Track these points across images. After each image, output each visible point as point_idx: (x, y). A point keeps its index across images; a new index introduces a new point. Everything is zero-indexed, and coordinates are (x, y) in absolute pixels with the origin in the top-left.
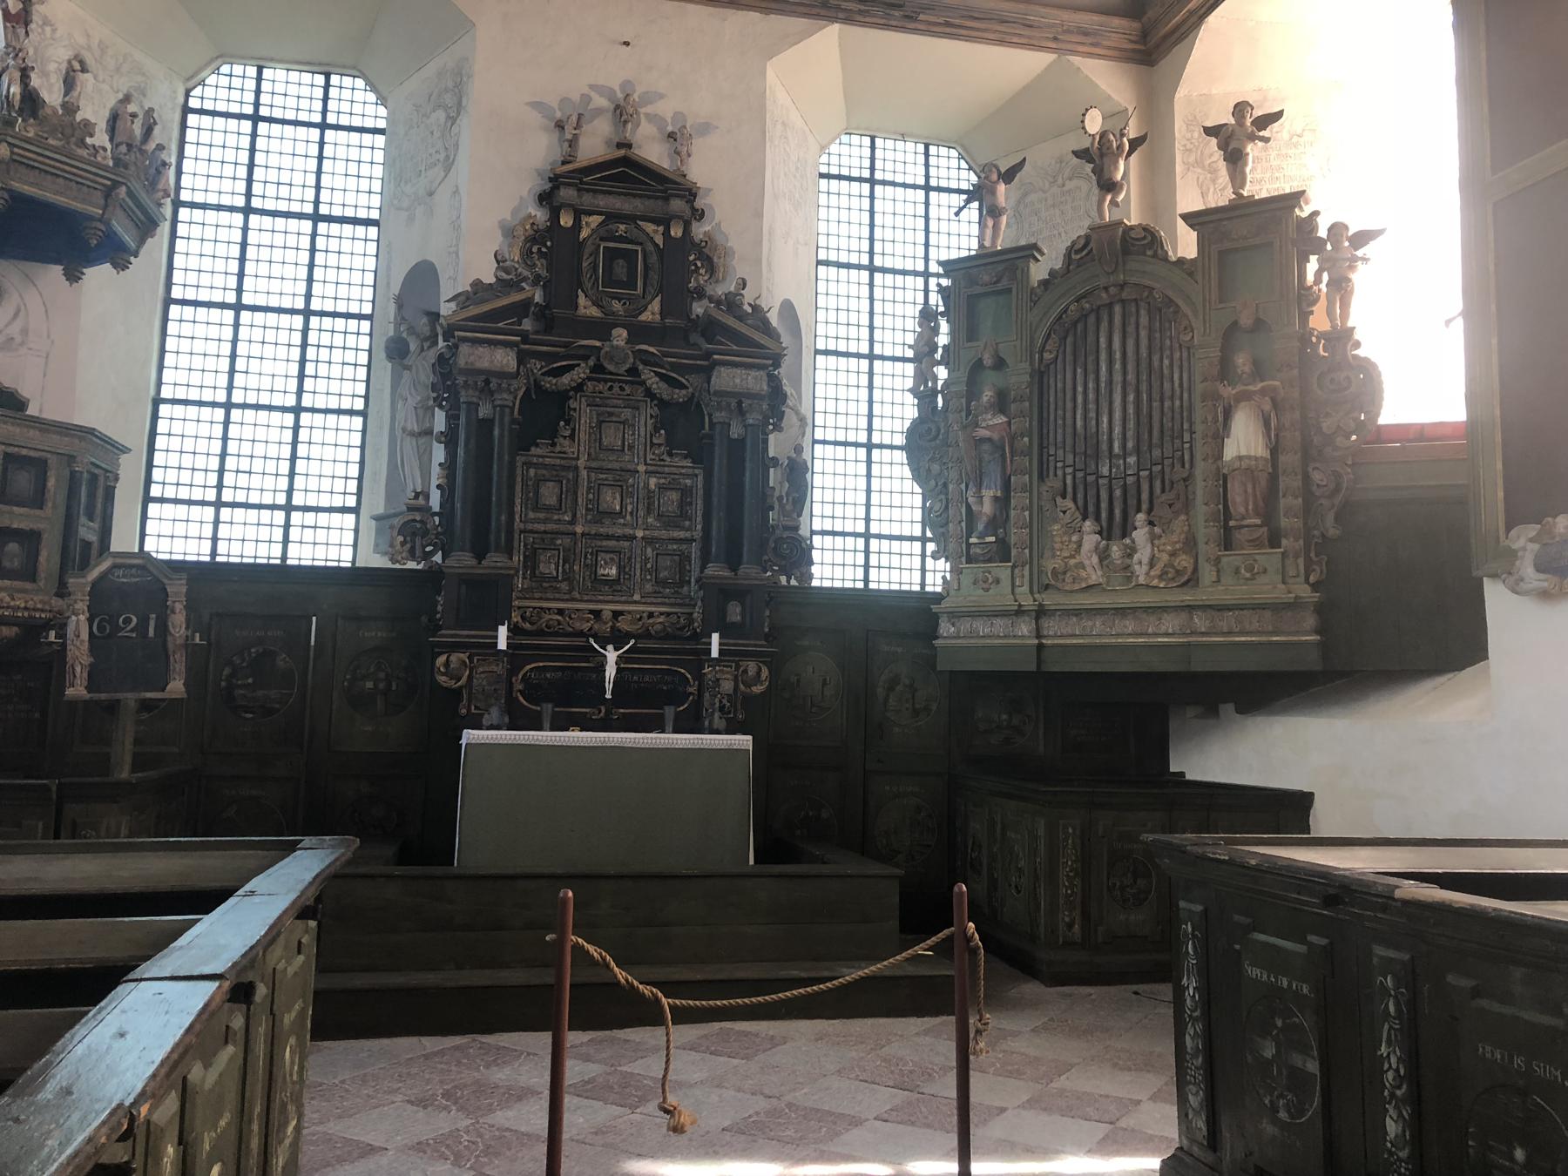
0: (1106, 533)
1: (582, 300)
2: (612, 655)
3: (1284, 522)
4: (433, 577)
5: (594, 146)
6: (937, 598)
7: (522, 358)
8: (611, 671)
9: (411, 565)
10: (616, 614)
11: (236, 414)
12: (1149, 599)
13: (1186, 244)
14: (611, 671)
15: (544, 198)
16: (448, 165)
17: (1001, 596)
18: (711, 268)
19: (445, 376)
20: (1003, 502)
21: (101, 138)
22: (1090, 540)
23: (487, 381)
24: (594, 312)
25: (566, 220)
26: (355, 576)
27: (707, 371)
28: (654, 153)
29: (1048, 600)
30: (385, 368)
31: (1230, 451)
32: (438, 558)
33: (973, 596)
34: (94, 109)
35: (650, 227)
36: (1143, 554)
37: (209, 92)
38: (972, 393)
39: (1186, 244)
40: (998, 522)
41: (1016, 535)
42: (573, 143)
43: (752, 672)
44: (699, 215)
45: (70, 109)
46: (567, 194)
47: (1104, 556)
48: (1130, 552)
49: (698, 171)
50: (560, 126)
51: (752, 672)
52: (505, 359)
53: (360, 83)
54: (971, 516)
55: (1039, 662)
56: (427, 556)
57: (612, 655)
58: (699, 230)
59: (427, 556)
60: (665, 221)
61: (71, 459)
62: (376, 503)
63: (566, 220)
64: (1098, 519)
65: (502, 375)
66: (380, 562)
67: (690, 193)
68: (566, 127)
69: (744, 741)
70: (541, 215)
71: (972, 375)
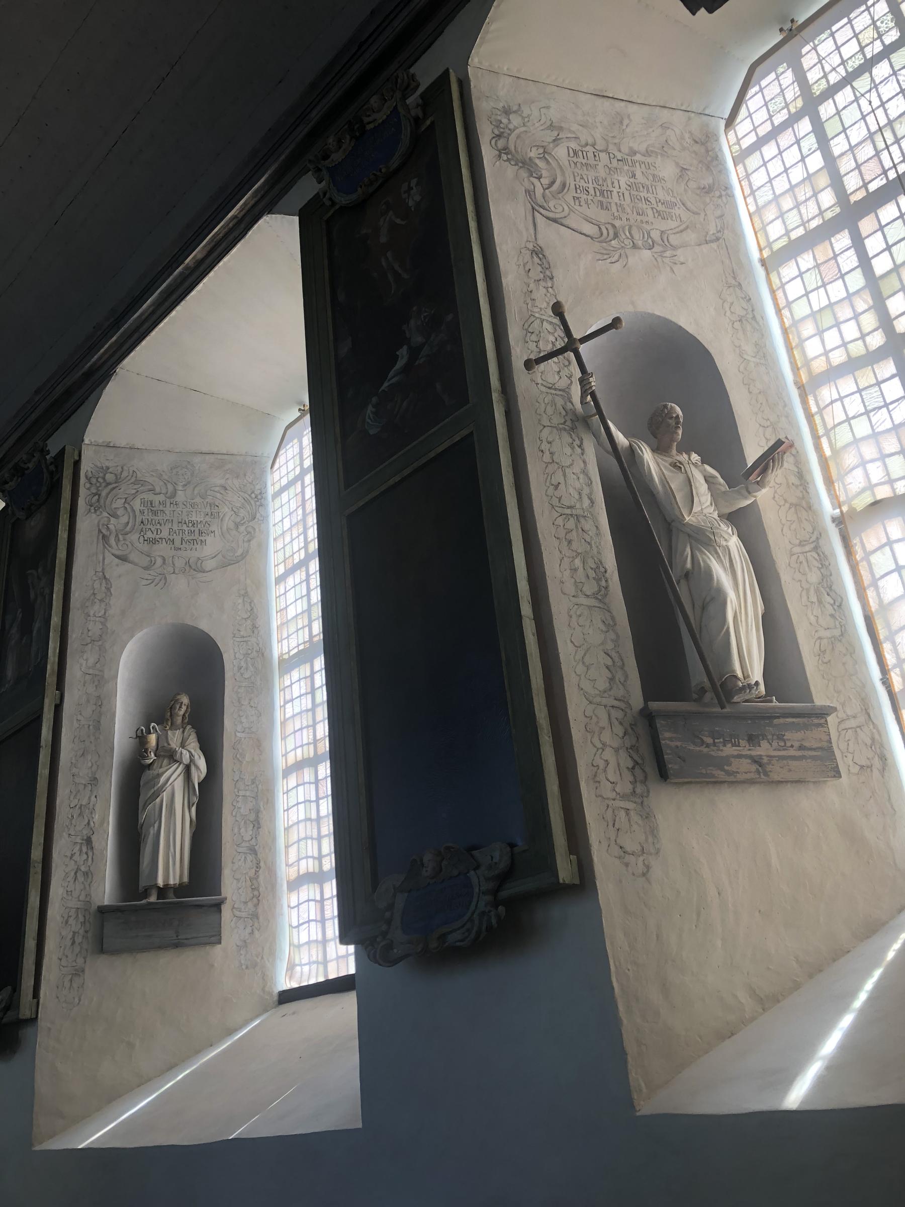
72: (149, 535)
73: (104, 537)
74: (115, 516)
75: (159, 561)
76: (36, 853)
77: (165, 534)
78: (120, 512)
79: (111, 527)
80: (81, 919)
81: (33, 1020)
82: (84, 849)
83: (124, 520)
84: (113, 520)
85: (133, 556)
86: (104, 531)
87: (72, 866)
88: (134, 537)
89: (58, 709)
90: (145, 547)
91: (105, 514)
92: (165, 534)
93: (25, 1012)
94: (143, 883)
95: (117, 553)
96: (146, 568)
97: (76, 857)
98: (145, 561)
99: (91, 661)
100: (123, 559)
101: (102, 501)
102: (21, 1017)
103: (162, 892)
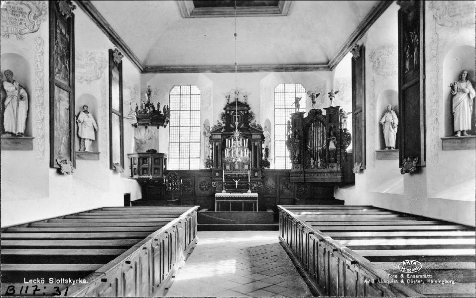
0: (315, 160)
1: (231, 125)
2: (237, 182)
3: (338, 159)
4: (211, 170)
5: (231, 101)
6: (290, 170)
7: (222, 136)
8: (237, 184)
9: (208, 169)
10: (238, 175)
11: (181, 144)
12: (319, 170)
13: (324, 113)
14: (237, 184)
15: (224, 109)
16: (210, 104)
17: (299, 170)
18: (251, 117)
19: (211, 139)
20: (300, 154)
21: (162, 113)
22: (312, 161)
23: (218, 140)
24: (233, 127)
25: (228, 112)
26: (201, 171)
27: (251, 135)
28: (242, 100)
29: (307, 170)
30: (203, 136)
31: (330, 147)
32: (211, 167)
33: (295, 170)
34: (161, 109)
35: (241, 112)
36: (319, 163)
37: (173, 92)
38: (295, 137)
39: (324, 113)
40: (299, 158)
41: (302, 160)
42: (228, 100)
43: (259, 183)
44: (250, 109)
45: (158, 110)
46: (228, 108)
47: (314, 163)
48: (318, 163)
49: (250, 102)
50: (226, 97)
51: (259, 183)
52: (219, 137)
53: (196, 86)
54: (295, 157)
55: (304, 180)
56: (210, 167)
57: (237, 182)
58: (250, 111)
59: (210, 167)
60: (244, 111)
61: (163, 158)
62: (202, 157)
63: (228, 112)
64: (314, 158)
65: (219, 139)
66: (203, 168)
67: (248, 106)
68: (228, 97)
69: (256, 195)
70: (224, 112)
71: (295, 133)
72: (452, 14)
73: (435, 18)
74: (438, 9)
75: (456, 23)
76: (422, 123)
77: (458, 12)
78: (441, 8)
79: (438, 14)
80: (436, 141)
81: (425, 166)
82: (435, 122)
83: (442, 10)
84: (438, 11)
85: (446, 24)
86: (435, 16)
87: (432, 127)
88: (446, 16)
89: (424, 80)
90: (450, 18)
91: (435, 10)
92: (458, 12)
93: (422, 164)
94: (456, 129)
95: (441, 23)
96: (451, 27)
97: (433, 124)
98: (450, 24)
99: (434, 64)
100: (442, 25)
101: (434, 5)
102: (422, 165)
103: (462, 133)
